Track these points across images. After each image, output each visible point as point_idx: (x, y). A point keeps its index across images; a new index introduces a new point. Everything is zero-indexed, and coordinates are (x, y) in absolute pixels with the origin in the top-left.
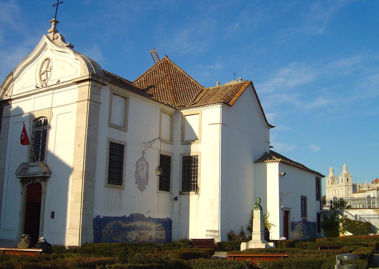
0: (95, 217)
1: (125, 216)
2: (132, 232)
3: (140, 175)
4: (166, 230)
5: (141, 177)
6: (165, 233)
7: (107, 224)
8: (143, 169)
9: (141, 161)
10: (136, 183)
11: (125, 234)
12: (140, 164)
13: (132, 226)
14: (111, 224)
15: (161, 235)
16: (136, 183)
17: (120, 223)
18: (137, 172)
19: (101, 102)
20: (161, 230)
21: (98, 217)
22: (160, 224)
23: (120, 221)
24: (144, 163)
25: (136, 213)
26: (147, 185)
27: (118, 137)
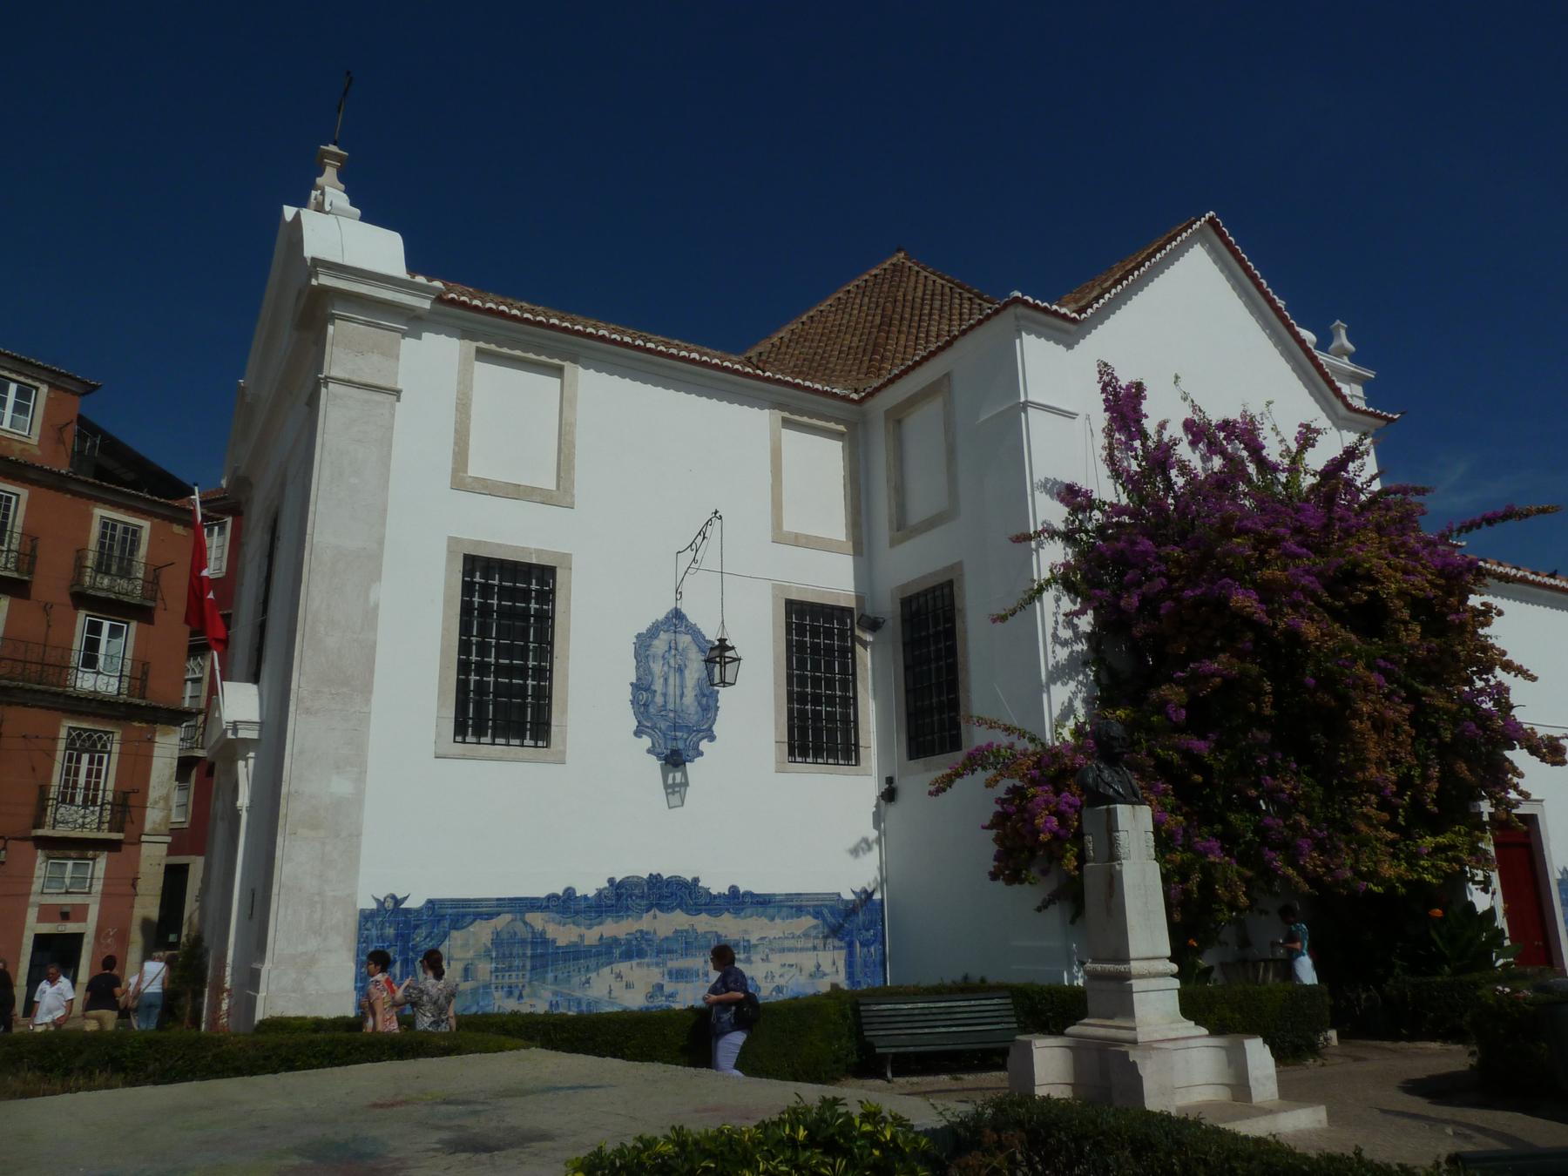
0: (374, 906)
1: (569, 892)
2: (623, 967)
3: (665, 695)
4: (850, 945)
5: (671, 706)
6: (841, 964)
7: (454, 933)
8: (680, 670)
9: (663, 636)
10: (638, 733)
11: (575, 980)
12: (660, 644)
13: (622, 936)
14: (482, 932)
15: (818, 972)
16: (638, 733)
17: (539, 926)
18: (641, 687)
19: (399, 387)
20: (815, 948)
21: (390, 905)
22: (808, 921)
23: (537, 920)
24: (685, 640)
25: (646, 876)
26: (712, 738)
27: (515, 532)
